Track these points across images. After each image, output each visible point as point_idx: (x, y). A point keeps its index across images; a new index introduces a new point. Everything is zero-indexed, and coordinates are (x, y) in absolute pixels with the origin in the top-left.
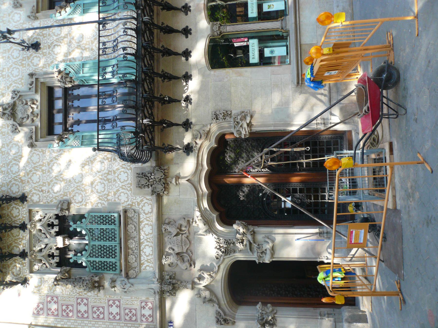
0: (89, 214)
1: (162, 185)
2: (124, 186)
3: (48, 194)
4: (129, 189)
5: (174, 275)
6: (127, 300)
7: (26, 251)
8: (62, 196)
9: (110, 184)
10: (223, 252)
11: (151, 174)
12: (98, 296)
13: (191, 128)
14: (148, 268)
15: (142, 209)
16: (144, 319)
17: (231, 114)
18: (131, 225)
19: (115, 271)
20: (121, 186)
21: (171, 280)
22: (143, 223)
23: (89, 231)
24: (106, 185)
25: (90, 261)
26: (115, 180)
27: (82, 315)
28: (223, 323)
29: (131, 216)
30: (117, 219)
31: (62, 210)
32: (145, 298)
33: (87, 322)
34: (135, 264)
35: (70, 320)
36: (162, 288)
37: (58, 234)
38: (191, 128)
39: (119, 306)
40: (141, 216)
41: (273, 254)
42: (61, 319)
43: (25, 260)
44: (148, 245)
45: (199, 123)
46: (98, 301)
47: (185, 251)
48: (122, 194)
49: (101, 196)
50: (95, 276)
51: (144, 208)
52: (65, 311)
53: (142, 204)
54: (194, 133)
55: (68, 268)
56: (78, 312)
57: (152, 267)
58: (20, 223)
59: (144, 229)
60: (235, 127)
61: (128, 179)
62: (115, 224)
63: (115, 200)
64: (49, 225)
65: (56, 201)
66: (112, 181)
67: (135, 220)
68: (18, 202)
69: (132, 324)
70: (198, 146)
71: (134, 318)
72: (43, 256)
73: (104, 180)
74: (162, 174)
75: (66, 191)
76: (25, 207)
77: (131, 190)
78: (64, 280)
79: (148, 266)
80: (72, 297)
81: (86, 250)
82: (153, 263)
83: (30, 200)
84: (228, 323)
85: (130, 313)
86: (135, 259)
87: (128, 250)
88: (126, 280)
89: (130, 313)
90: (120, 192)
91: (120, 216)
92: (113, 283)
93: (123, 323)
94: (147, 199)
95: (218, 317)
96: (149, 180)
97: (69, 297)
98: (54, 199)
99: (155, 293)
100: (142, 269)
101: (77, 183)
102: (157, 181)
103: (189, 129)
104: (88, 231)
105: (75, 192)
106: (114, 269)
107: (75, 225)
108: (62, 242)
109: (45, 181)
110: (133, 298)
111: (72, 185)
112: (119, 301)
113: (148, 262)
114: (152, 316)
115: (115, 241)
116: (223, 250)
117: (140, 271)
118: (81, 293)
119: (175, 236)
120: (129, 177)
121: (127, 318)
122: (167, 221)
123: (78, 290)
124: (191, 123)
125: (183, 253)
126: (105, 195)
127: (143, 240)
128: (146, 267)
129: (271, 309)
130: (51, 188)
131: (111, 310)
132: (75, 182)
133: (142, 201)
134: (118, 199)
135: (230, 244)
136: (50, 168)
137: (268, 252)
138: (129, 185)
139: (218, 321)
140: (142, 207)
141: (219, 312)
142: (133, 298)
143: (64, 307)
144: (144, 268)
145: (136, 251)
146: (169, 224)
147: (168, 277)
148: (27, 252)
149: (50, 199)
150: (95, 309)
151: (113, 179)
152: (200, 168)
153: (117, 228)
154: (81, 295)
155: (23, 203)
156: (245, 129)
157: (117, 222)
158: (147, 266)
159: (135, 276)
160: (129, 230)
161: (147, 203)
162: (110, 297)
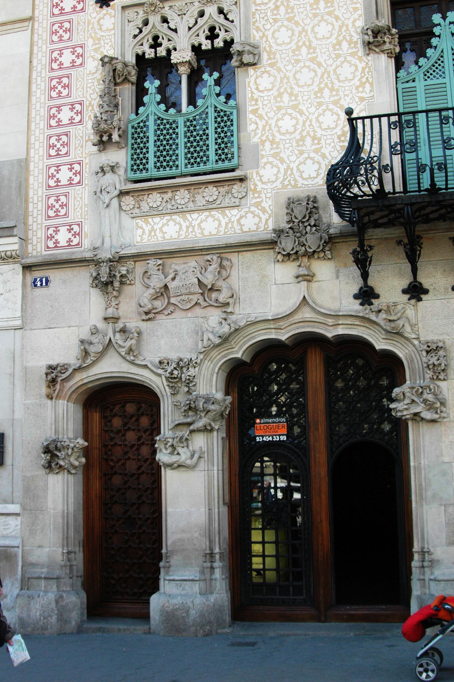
0: (232, 107)
1: (293, 249)
2: (292, 173)
3: (271, 21)
4: (286, 183)
5: (128, 282)
6: (81, 198)
8: (268, 49)
9: (294, 144)
10: (171, 373)
11: (315, 225)
12: (87, 141)
13: (409, 299)
14: (140, 232)
15: (247, 213)
16: (51, 231)
17: (440, 380)
18: (217, 193)
19: (132, 170)
20: (292, 165)
21: (118, 279)
24: (293, 136)
25: (148, 120)
26: (301, 153)
27: (54, 116)
28: (49, 377)
29: (234, 191)
30: (227, 165)
31: (240, 53)
32: (86, 230)
33: (42, 127)
34: (145, 207)
35: (45, 94)
36: (103, 262)
37: (196, 49)
38: (409, 299)
39: (71, 184)
40: (235, 211)
41: (170, 466)
42: (45, 77)
44: (181, 228)
45: (420, 315)
46: (78, 142)
47: (173, 300)
48: (275, 170)
49: (270, 129)
50: (120, 132)
51: (250, 216)
52: (59, 83)
53: (257, 212)
54: (399, 307)
55: (134, 79)
56: (58, 107)
57: (142, 239)
59: (210, 219)
60: (413, 388)
61: (306, 179)
62: (217, 161)
63: (263, 156)
64: (212, 29)
65: (257, 38)
66: (300, 148)
67: (227, 200)
69: (42, 210)
70: (373, 317)
71: (51, 213)
72: (154, 26)
73: (303, 131)
74: (314, 249)
75: (278, 56)
77: (284, 187)
78: (111, 74)
79: (144, 232)
80: (83, 94)
81: (167, 111)
82: (149, 240)
84: (49, 387)
85: (60, 206)
86: (155, 206)
87: (170, 191)
88: (117, 192)
89: (60, 206)
90: (280, 165)
91: (233, 170)
93: (43, 193)
94: (267, 221)
95: (59, 369)
96: (303, 222)
97: (83, 88)
98: (261, 34)
99: (95, 249)
100: (137, 221)
101: (294, 75)
102: (301, 239)
103: (408, 296)
104: (203, 109)
105: (277, 74)
107: (213, 83)
108: (181, 60)
109: (295, 10)
110: (86, 209)
111: (290, 67)
112: (79, 182)
113: (150, 232)
114: (56, 247)
115: (186, 165)
116: (176, 372)
117: (133, 218)
118: (90, 108)
119: (199, 280)
120: (310, 182)
121: (52, 201)
122: (225, 263)
124: (420, 300)
125: (169, 298)
126: (273, 135)
127: (190, 220)
128: (142, 228)
129: (76, 463)
130: (283, 25)
131: (64, 169)
132: (296, 73)
133: (264, 210)
134: (266, 164)
135: (188, 385)
136: (322, 17)
137: (174, 459)
138: (293, 183)
139: (51, 368)
140: (252, 213)
141: (67, 369)
142: (86, 209)
143: (65, 81)
144: (140, 225)
145: (169, 206)
146: (221, 266)
147: (124, 272)
150: (64, 138)
151: (304, 148)
152: (330, 321)
153: (210, 166)
154: (87, 110)
156: (406, 409)
157: (221, 165)
158: (144, 230)
160: (206, 190)
161: (260, 220)
162: (86, 164)
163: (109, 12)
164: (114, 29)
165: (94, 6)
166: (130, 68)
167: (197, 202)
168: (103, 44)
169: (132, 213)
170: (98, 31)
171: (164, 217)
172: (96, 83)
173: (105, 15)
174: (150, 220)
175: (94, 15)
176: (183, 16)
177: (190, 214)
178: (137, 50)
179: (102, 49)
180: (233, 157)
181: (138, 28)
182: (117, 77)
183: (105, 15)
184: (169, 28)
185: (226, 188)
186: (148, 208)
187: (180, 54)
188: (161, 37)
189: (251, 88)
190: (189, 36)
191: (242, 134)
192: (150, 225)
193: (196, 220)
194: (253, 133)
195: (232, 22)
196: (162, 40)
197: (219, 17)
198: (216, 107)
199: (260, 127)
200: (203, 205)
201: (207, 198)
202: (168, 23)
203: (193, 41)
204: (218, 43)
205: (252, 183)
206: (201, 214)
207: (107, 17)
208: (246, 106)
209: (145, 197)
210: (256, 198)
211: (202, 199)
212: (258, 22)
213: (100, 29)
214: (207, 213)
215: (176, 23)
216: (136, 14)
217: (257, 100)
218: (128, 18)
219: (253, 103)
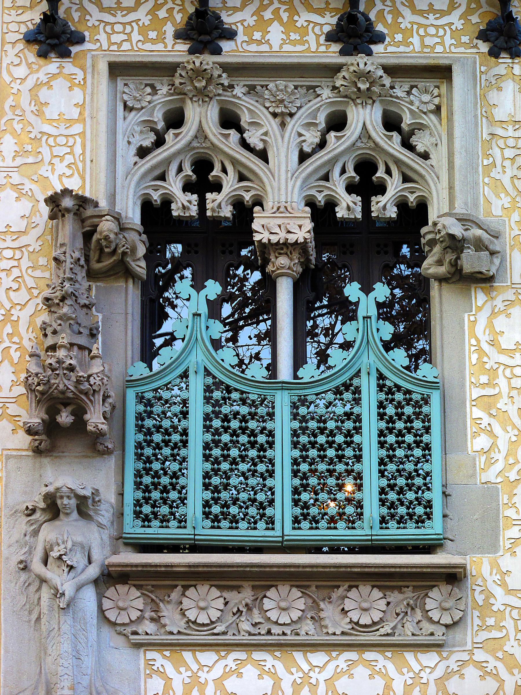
0: (433, 385)
7: (226, 46)
15: (463, 664)
18: (382, 604)
19: (137, 514)
22: (391, 668)
23: (347, 386)
29: (430, 604)
43: (178, 36)
50: (108, 408)
51: (471, 672)
58: (372, 16)
59: (361, 672)
62: (383, 520)
65: (497, 211)
67: (410, 627)
68: (486, 8)
76: (460, 44)
83: (501, 69)
86: (203, 619)
88: (93, 571)
92: (73, 502)
100: (150, 655)
104: (345, 378)
106: (147, 509)
107: (373, 312)
108: (281, 236)
115: (296, 520)
117: (138, 646)
123: (24, 315)
128: (162, 674)
140: (480, 665)
145: (245, 626)
148: (218, 51)
149: (506, 180)
155: (483, 36)
159: (112, 615)
160: (353, 593)
163: (66, 71)
164: (81, 119)
165: (21, 46)
166: (133, 236)
167: (327, 622)
168: (47, 158)
169: (135, 633)
170: (32, 118)
171: (229, 652)
172: (25, 263)
173: (54, 76)
174: (187, 655)
175: (21, 71)
176: (288, 119)
177: (305, 653)
178: (150, 191)
179: (44, 171)
180: (429, 516)
181: (152, 130)
182: (94, 256)
183: (54, 76)
184: (244, 144)
185: (409, 593)
186: (182, 625)
187: (279, 221)
188: (217, 167)
189: (478, 340)
190: (304, 175)
191: (452, 458)
192: (188, 668)
193: (322, 668)
194: (483, 459)
195: (425, 156)
196: (222, 175)
197: (390, 138)
198: (381, 377)
199: (502, 444)
200: (343, 633)
201: (354, 616)
202: (240, 130)
203: (313, 192)
204: (384, 208)
205: (478, 589)
206: (334, 654)
207: (60, 84)
208: (463, 386)
209: (175, 595)
210: (489, 628)
211: (338, 616)
212: (499, 168)
213: (39, 113)
214: (353, 655)
215: (266, 134)
216: (148, 90)
217: (493, 372)
218: (126, 97)
219: (484, 379)
